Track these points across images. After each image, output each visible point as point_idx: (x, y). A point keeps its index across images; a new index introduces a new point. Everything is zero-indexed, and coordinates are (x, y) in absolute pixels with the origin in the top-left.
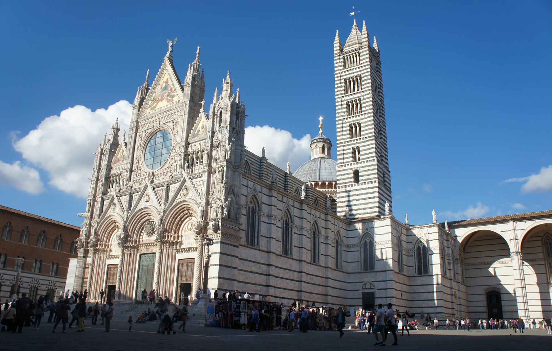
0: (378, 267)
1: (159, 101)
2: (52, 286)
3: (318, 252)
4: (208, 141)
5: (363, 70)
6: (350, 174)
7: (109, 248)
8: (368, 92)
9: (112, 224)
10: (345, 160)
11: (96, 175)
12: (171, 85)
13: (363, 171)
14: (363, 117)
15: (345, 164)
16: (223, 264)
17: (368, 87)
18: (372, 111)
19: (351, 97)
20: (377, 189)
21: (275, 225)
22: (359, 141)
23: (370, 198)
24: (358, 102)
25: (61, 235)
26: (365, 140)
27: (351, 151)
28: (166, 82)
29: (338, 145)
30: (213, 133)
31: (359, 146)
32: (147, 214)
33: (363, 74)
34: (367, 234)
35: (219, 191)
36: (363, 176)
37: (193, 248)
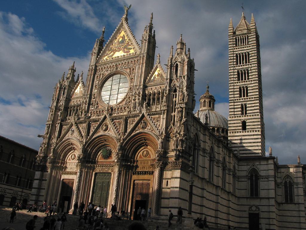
0: (263, 194)
1: (117, 51)
2: (3, 192)
3: (225, 180)
4: (166, 87)
5: (251, 49)
6: (239, 123)
7: (65, 165)
8: (255, 65)
9: (69, 146)
10: (235, 113)
11: (55, 104)
12: (128, 40)
13: (249, 122)
14: (250, 82)
15: (235, 116)
19: (240, 67)
20: (260, 137)
21: (207, 157)
23: (254, 143)
24: (246, 71)
25: (13, 150)
26: (251, 99)
27: (240, 106)
28: (122, 37)
30: (171, 80)
31: (246, 103)
32: (105, 140)
35: (178, 127)
36: (249, 125)
37: (150, 172)
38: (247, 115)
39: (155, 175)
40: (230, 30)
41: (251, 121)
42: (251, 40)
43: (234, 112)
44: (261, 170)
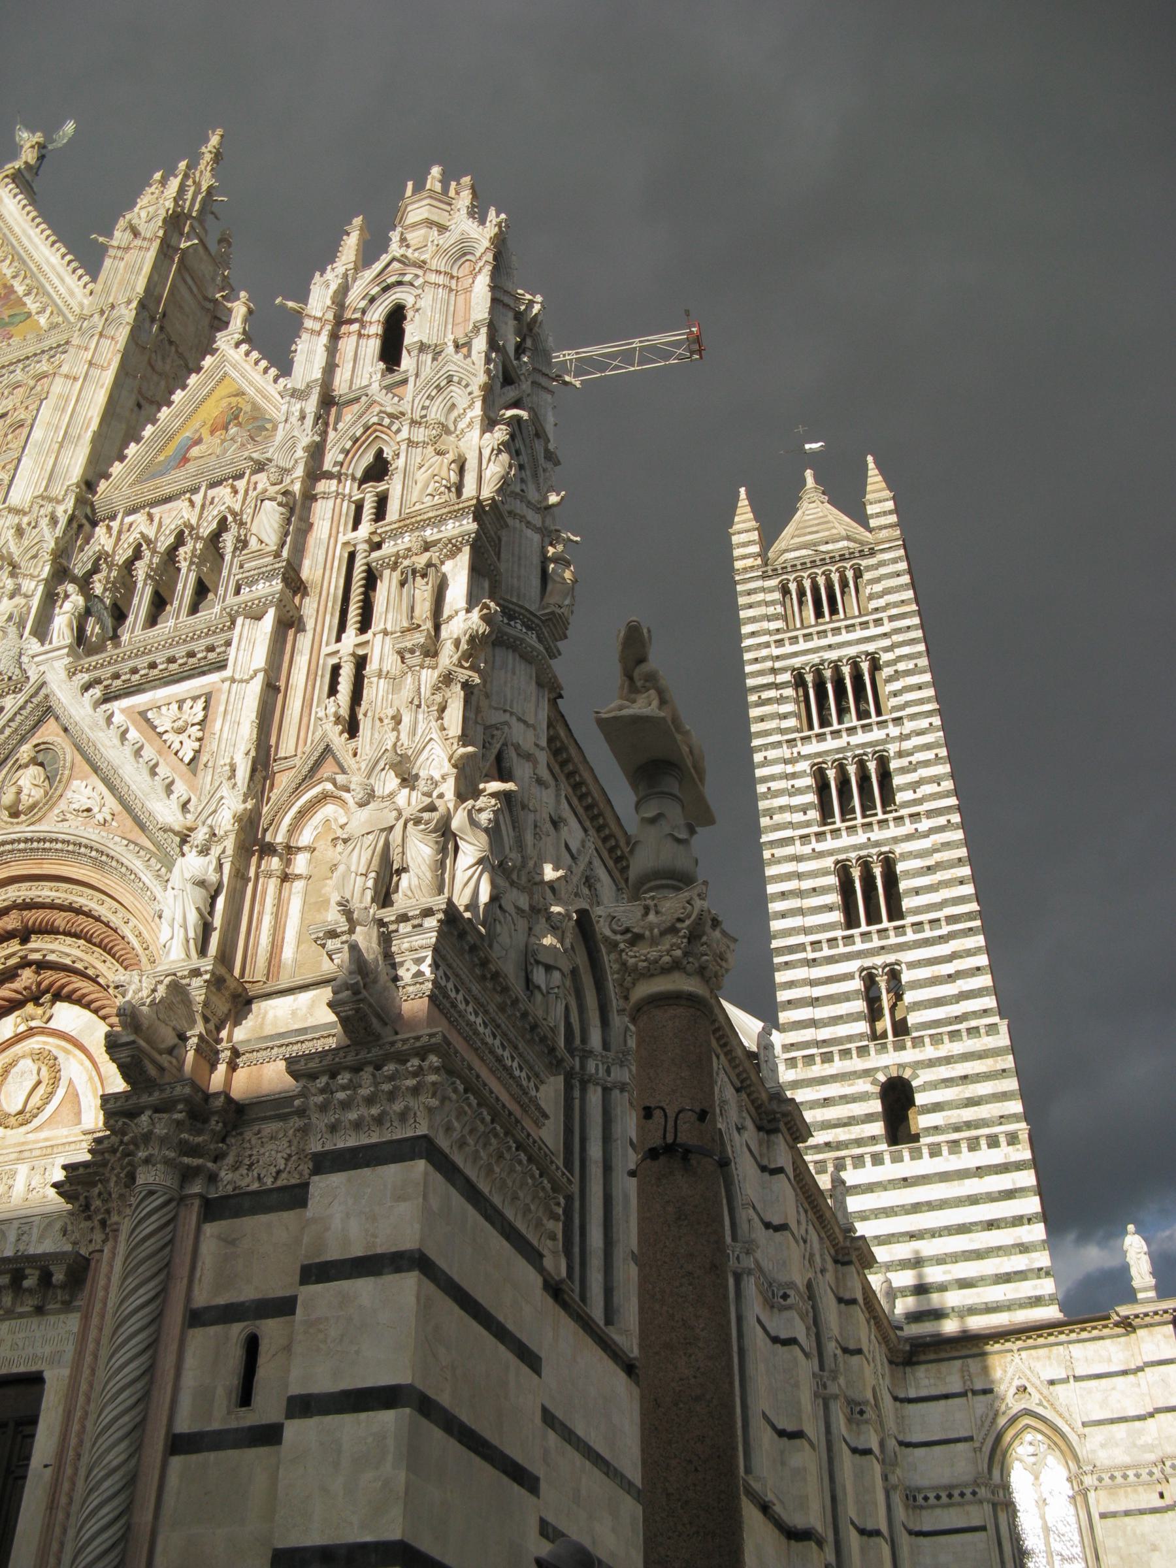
5: (885, 635)
8: (924, 723)
14: (908, 828)
16: (444, 1399)
17: (921, 702)
18: (953, 801)
19: (830, 744)
22: (893, 940)
23: (991, 1225)
24: (872, 766)
26: (928, 933)
27: (857, 984)
29: (777, 960)
31: (898, 963)
33: (887, 650)
34: (1027, 1421)
36: (937, 1107)
38: (915, 1034)
39: (102, 1282)
40: (745, 545)
41: (944, 1072)
42: (878, 588)
43: (813, 1023)
44: (1084, 1424)
